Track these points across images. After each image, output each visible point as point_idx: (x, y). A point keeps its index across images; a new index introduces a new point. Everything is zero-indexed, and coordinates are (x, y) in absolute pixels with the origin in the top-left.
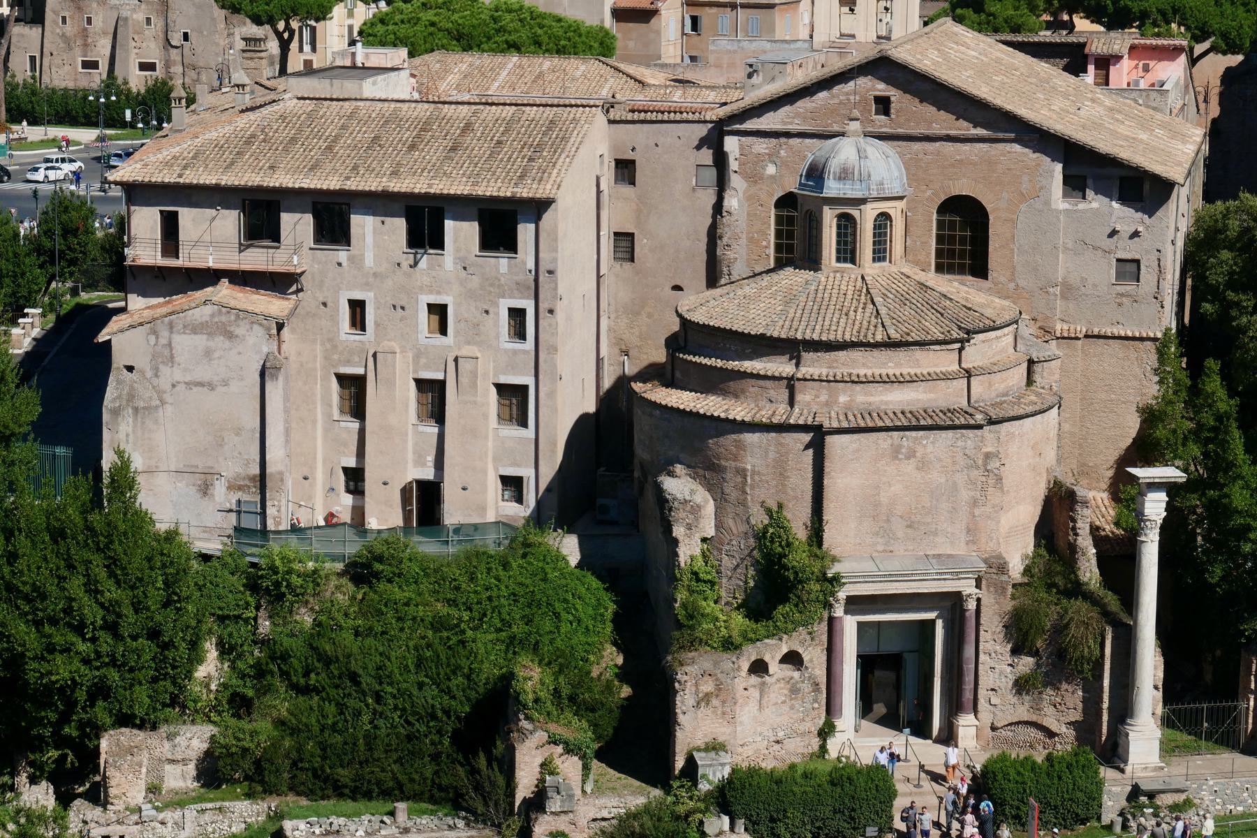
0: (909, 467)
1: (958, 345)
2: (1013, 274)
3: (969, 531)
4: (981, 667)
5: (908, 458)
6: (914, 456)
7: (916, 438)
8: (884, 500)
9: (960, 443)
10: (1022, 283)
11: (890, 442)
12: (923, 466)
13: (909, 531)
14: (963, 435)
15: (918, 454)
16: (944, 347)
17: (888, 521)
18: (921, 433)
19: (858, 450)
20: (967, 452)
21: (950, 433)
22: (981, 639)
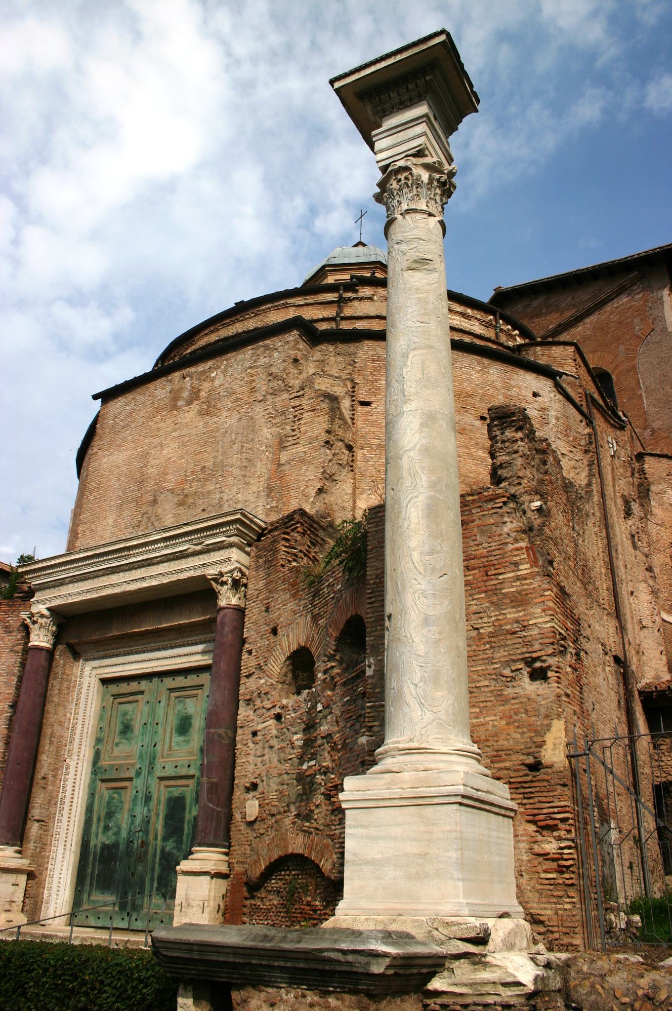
0: (189, 415)
1: (331, 297)
2: (646, 420)
3: (270, 489)
5: (189, 403)
6: (198, 398)
7: (204, 372)
8: (152, 471)
9: (263, 360)
10: (656, 425)
11: (168, 389)
13: (181, 511)
14: (266, 347)
15: (203, 394)
17: (155, 502)
18: (210, 363)
19: (130, 414)
20: (273, 370)
22: (244, 672)
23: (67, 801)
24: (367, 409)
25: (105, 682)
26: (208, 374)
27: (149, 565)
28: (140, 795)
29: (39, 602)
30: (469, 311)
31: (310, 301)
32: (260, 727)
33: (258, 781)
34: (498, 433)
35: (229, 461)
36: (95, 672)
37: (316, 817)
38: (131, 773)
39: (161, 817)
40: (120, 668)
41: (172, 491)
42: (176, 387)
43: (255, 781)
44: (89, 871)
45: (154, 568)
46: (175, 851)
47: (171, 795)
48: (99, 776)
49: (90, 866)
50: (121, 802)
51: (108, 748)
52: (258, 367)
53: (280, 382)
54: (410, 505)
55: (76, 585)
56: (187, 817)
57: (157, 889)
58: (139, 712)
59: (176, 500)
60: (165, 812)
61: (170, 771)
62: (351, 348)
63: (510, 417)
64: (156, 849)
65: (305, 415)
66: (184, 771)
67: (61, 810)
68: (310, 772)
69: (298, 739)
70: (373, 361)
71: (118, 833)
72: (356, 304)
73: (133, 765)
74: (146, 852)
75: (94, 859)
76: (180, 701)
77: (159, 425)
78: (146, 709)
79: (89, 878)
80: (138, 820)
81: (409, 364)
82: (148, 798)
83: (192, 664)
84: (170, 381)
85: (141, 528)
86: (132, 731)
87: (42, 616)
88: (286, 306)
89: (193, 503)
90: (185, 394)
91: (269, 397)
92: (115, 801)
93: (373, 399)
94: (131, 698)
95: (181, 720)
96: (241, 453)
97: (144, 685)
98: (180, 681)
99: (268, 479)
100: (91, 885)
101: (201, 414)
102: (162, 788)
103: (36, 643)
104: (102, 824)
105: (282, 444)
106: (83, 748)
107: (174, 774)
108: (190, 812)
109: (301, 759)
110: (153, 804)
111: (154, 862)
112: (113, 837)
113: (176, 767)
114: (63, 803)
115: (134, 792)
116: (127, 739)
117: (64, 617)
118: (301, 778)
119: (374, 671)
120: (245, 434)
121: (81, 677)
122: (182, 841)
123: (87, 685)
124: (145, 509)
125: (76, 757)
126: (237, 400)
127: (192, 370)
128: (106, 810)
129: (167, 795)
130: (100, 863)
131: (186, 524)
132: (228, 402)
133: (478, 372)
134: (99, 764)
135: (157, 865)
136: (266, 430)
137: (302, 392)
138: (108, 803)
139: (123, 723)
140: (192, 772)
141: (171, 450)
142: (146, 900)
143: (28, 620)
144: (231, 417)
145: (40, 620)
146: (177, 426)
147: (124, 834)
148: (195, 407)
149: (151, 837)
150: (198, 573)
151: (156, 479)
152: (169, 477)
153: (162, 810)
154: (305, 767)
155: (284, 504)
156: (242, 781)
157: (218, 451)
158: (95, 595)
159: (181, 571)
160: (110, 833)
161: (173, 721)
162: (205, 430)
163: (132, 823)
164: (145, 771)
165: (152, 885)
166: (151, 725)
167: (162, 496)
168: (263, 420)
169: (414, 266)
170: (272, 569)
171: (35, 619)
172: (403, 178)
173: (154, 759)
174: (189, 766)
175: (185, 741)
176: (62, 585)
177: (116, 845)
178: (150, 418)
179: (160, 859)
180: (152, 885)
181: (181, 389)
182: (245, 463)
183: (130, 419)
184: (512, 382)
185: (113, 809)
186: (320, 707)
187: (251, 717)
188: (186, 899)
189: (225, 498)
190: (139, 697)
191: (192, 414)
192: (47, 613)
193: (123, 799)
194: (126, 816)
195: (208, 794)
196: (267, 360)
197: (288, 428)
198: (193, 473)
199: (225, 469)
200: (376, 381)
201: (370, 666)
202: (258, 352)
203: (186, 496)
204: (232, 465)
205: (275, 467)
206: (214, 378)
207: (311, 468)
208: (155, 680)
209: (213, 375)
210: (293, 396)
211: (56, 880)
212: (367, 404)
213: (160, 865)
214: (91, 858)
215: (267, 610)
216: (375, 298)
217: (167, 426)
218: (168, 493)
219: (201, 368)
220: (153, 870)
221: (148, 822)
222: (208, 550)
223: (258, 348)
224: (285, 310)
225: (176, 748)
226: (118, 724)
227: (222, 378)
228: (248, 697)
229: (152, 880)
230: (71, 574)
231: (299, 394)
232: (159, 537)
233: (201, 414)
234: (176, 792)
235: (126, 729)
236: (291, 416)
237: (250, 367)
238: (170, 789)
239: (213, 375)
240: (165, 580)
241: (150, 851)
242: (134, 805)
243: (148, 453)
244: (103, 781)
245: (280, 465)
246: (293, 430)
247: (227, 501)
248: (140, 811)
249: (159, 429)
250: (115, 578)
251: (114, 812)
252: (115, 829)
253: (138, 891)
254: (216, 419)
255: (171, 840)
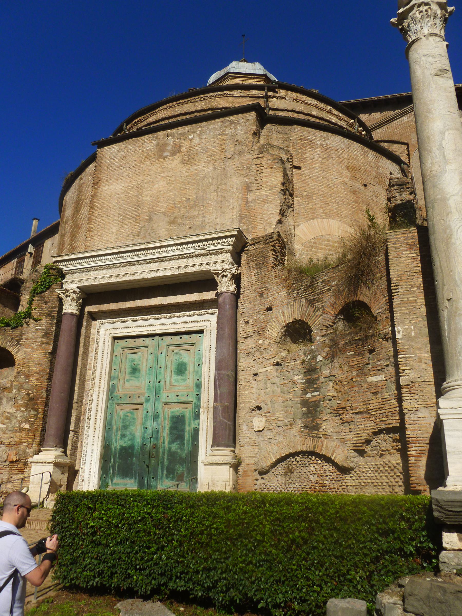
0: (174, 163)
4: (241, 376)
5: (173, 154)
6: (180, 151)
7: (183, 134)
8: (146, 198)
9: (229, 131)
11: (155, 142)
12: (190, 159)
13: (172, 227)
14: (232, 122)
15: (184, 149)
16: (244, 93)
17: (150, 219)
18: (188, 128)
19: (125, 157)
20: (238, 137)
21: (218, 123)
23: (92, 418)
24: (299, 171)
25: (115, 338)
26: (186, 136)
27: (162, 261)
28: (150, 414)
29: (70, 282)
30: (341, 115)
31: (243, 94)
32: (260, 371)
33: (262, 405)
34: (397, 194)
35: (208, 196)
36: (108, 332)
37: (324, 427)
38: (143, 399)
39: (166, 428)
40: (130, 330)
41: (164, 214)
42: (162, 142)
43: (259, 405)
44: (112, 464)
45: (166, 263)
46: (179, 451)
47: (173, 414)
48: (116, 402)
49: (112, 461)
50: (134, 419)
51: (121, 383)
52: (226, 135)
53: (244, 147)
54: (459, 231)
55: (101, 272)
56: (187, 428)
57: (166, 475)
58: (144, 360)
59: (168, 219)
60: (169, 425)
61: (173, 398)
62: (286, 128)
63: (406, 185)
64: (164, 450)
65: (264, 171)
66: (184, 399)
67: (88, 424)
68: (315, 399)
69: (300, 379)
70: (301, 140)
71: (133, 439)
72: (274, 100)
73: (143, 394)
74: (157, 452)
75: (115, 456)
76: (176, 353)
77: (150, 168)
78: (151, 357)
79: (111, 469)
80: (149, 431)
81: (446, 138)
82: (156, 416)
83: (187, 329)
84: (157, 138)
85: (140, 237)
86: (139, 372)
87: (74, 292)
88: (227, 96)
89: (182, 223)
90: (169, 148)
91: (236, 156)
92: (129, 418)
93: (302, 165)
94: (137, 350)
95: (179, 365)
96: (217, 192)
97: (148, 341)
98: (176, 339)
99: (240, 211)
100: (113, 473)
101: (183, 162)
102: (166, 410)
103: (70, 311)
104: (120, 433)
105: (248, 188)
106: (103, 383)
107: (176, 401)
108: (189, 425)
109: (305, 392)
110: (160, 420)
111: (163, 458)
112: (129, 442)
113: (177, 396)
114: (89, 419)
115: (145, 412)
116: (136, 377)
117: (86, 294)
118: (305, 403)
119: (403, 335)
120: (219, 179)
121: (98, 335)
122: (184, 444)
123: (103, 340)
124: (142, 224)
125: (98, 389)
126: (211, 156)
127: (173, 131)
128: (121, 424)
129: (170, 414)
130: (119, 459)
131: (195, 235)
132: (205, 157)
133: (362, 155)
134: (115, 394)
135: (166, 460)
136: (235, 178)
137: (261, 155)
138: (123, 420)
139: (132, 367)
140: (190, 399)
141: (160, 185)
142: (159, 482)
143: (62, 295)
144: (208, 167)
145: (72, 295)
146: (164, 170)
147: (138, 440)
148: (178, 158)
149: (160, 441)
150: (203, 268)
151: (150, 205)
152: (160, 204)
153: (167, 424)
154: (309, 396)
155: (253, 228)
156: (247, 405)
157: (199, 189)
158: (118, 280)
159: (189, 266)
160: (126, 439)
161: (172, 366)
162: (188, 174)
163: (145, 432)
164: (152, 399)
165: (162, 473)
166: (155, 368)
167: (156, 217)
168: (233, 171)
169: (440, 73)
170: (264, 269)
171: (68, 294)
172: (424, 10)
173: (160, 390)
174: (187, 395)
175: (182, 379)
176: (89, 271)
177: (132, 447)
178: (142, 162)
179: (168, 456)
180: (162, 473)
181: (165, 145)
182: (220, 199)
183: (124, 162)
184: (380, 164)
185: (128, 423)
186: (320, 358)
187: (251, 365)
188: (212, 481)
189: (207, 221)
190: (144, 350)
191: (175, 162)
192: (78, 290)
193: (135, 417)
194: (139, 427)
195: (222, 414)
196: (233, 130)
197: (252, 178)
198: (180, 202)
199: (205, 202)
200: (304, 153)
201: (399, 332)
202: (226, 125)
203: (175, 218)
204: (210, 200)
205: (244, 203)
206: (192, 139)
207: (272, 206)
208: (157, 337)
209: (190, 137)
210: (255, 157)
211: (87, 470)
212: (298, 168)
213: (168, 459)
214: (113, 455)
215: (261, 295)
216: (287, 98)
217: (155, 168)
218: (161, 215)
219: (180, 130)
220: (163, 463)
221: (158, 432)
222: (210, 254)
223: (225, 122)
224: (225, 99)
225: (175, 384)
226: (128, 367)
227: (198, 140)
228: (248, 352)
229: (162, 469)
230: (98, 265)
231: (259, 156)
232: (172, 242)
233: (183, 162)
234: (177, 413)
235: (135, 370)
236: (255, 171)
237: (220, 134)
238: (173, 410)
239: (190, 137)
240: (177, 272)
241: (161, 450)
242: (145, 421)
243: (141, 186)
244: (119, 404)
245: (247, 202)
246: (257, 180)
247: (209, 223)
248: (151, 425)
249: (149, 170)
250: (134, 269)
251: (128, 426)
252: (130, 437)
253: (152, 477)
254: (195, 168)
255: (175, 444)
